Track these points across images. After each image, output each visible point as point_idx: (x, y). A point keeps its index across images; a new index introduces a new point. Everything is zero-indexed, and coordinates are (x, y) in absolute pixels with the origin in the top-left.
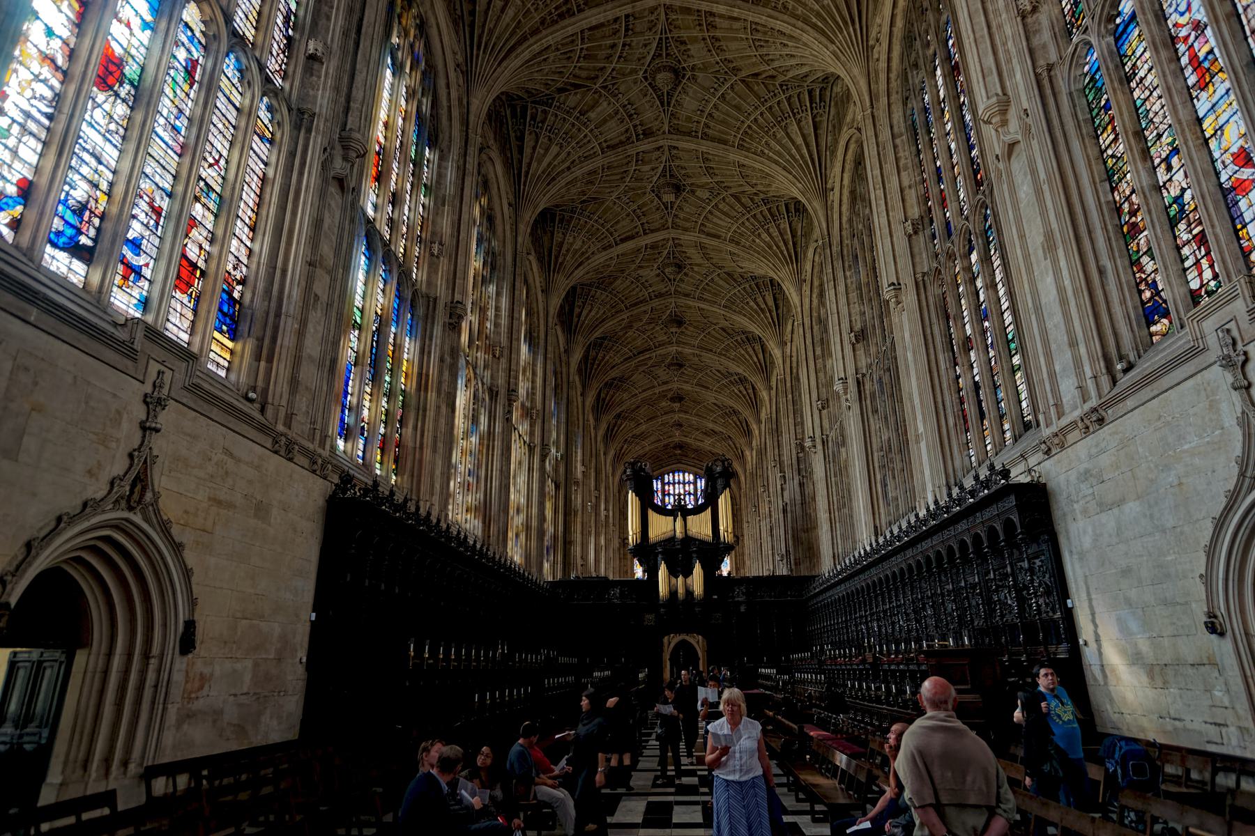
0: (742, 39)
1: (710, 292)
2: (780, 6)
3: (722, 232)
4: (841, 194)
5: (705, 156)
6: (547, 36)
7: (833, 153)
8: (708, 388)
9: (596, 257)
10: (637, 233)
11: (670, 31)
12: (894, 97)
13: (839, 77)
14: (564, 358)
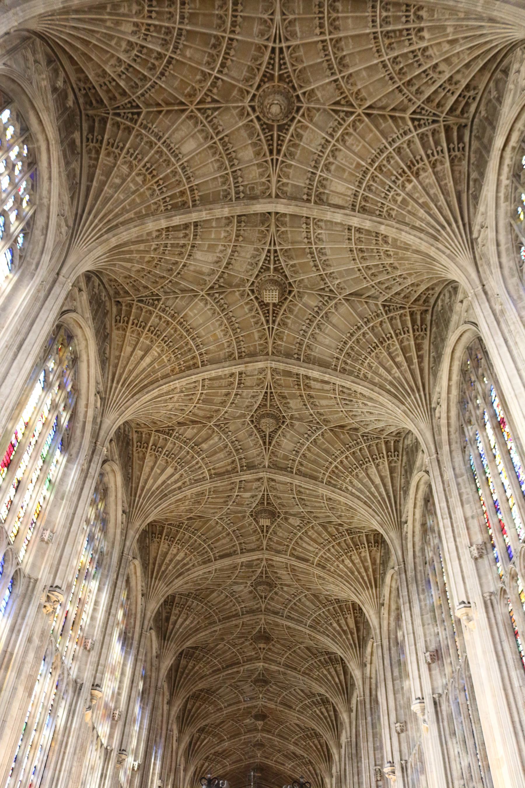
0: (331, 398)
1: (296, 611)
2: (361, 376)
3: (310, 556)
4: (414, 527)
5: (299, 489)
6: (175, 380)
7: (406, 492)
8: (291, 707)
9: (196, 569)
10: (235, 551)
11: (275, 388)
12: (454, 446)
13: (410, 431)
14: (155, 662)
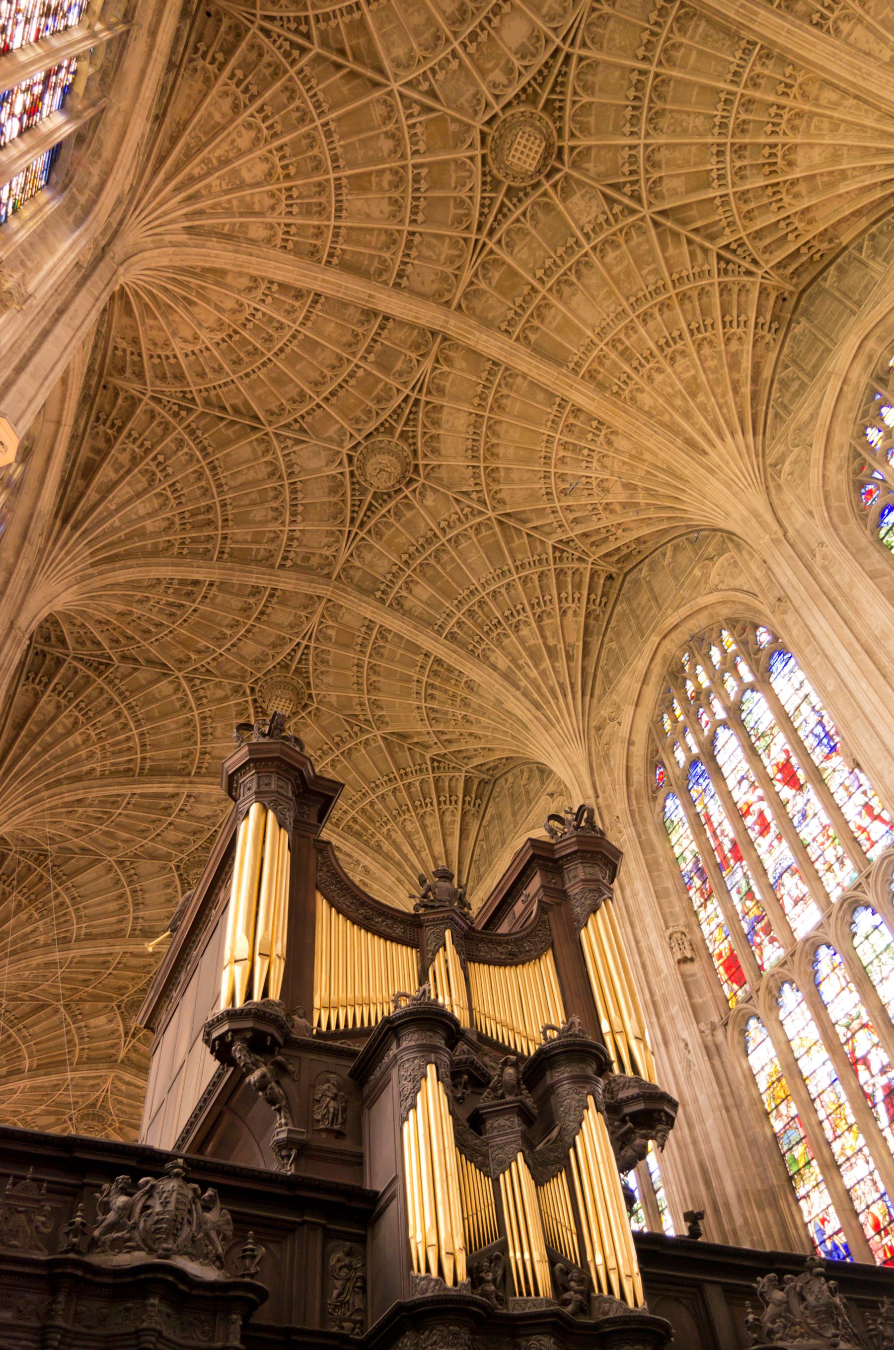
1: (431, 582)
